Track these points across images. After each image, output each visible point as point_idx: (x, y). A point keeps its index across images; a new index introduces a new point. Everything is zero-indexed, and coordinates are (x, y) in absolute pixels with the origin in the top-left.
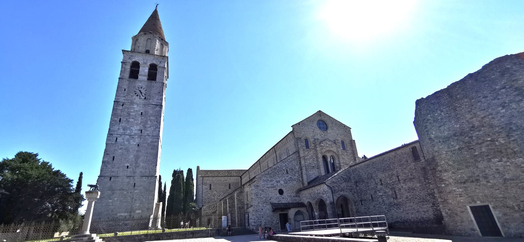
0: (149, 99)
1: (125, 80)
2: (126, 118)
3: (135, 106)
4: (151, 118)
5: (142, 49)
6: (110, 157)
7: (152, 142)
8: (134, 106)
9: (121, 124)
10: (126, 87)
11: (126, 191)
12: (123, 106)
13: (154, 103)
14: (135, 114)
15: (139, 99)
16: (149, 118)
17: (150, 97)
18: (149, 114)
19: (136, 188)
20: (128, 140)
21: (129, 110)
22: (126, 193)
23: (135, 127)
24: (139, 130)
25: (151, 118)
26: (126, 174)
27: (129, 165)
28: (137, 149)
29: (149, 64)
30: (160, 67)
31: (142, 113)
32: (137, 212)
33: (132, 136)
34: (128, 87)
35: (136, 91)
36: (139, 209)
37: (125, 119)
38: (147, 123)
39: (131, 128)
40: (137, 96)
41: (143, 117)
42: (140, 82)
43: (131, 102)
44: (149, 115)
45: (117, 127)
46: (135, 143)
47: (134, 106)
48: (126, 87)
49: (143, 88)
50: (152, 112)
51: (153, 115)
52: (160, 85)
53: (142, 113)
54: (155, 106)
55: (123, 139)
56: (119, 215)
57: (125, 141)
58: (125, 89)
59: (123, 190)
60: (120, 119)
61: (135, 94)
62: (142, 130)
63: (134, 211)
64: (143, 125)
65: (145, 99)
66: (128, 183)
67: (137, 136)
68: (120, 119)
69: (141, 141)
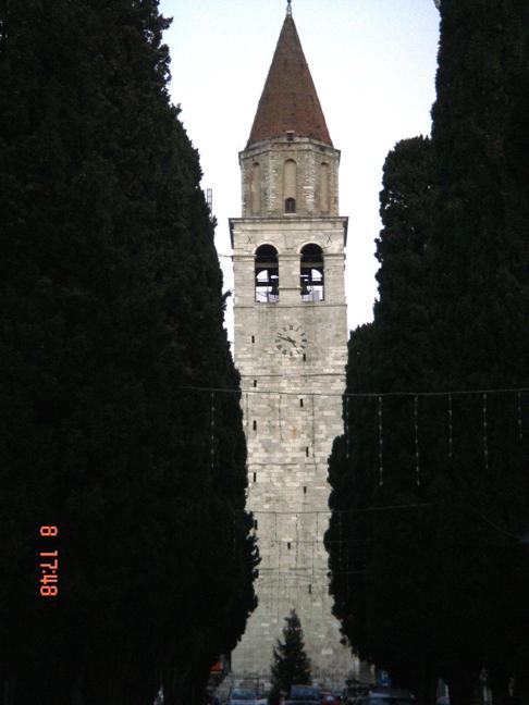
0: (317, 359)
1: (248, 310)
3: (284, 384)
4: (326, 413)
5: (275, 202)
8: (282, 385)
9: (258, 437)
10: (254, 330)
12: (255, 385)
13: (327, 371)
15: (289, 363)
17: (317, 353)
19: (314, 596)
20: (281, 479)
23: (291, 440)
24: (301, 449)
25: (326, 413)
27: (290, 540)
28: (301, 501)
29: (298, 251)
30: (329, 255)
32: (324, 652)
33: (289, 467)
34: (259, 331)
36: (327, 648)
37: (265, 423)
39: (283, 445)
40: (284, 352)
41: (304, 414)
42: (284, 310)
43: (273, 371)
46: (297, 485)
47: (282, 385)
48: (254, 330)
49: (295, 328)
52: (337, 313)
53: (301, 400)
54: (330, 377)
55: (269, 474)
57: (274, 480)
60: (255, 422)
61: (279, 347)
64: (308, 436)
65: (304, 358)
67: (298, 466)
68: (255, 422)
69: (309, 480)
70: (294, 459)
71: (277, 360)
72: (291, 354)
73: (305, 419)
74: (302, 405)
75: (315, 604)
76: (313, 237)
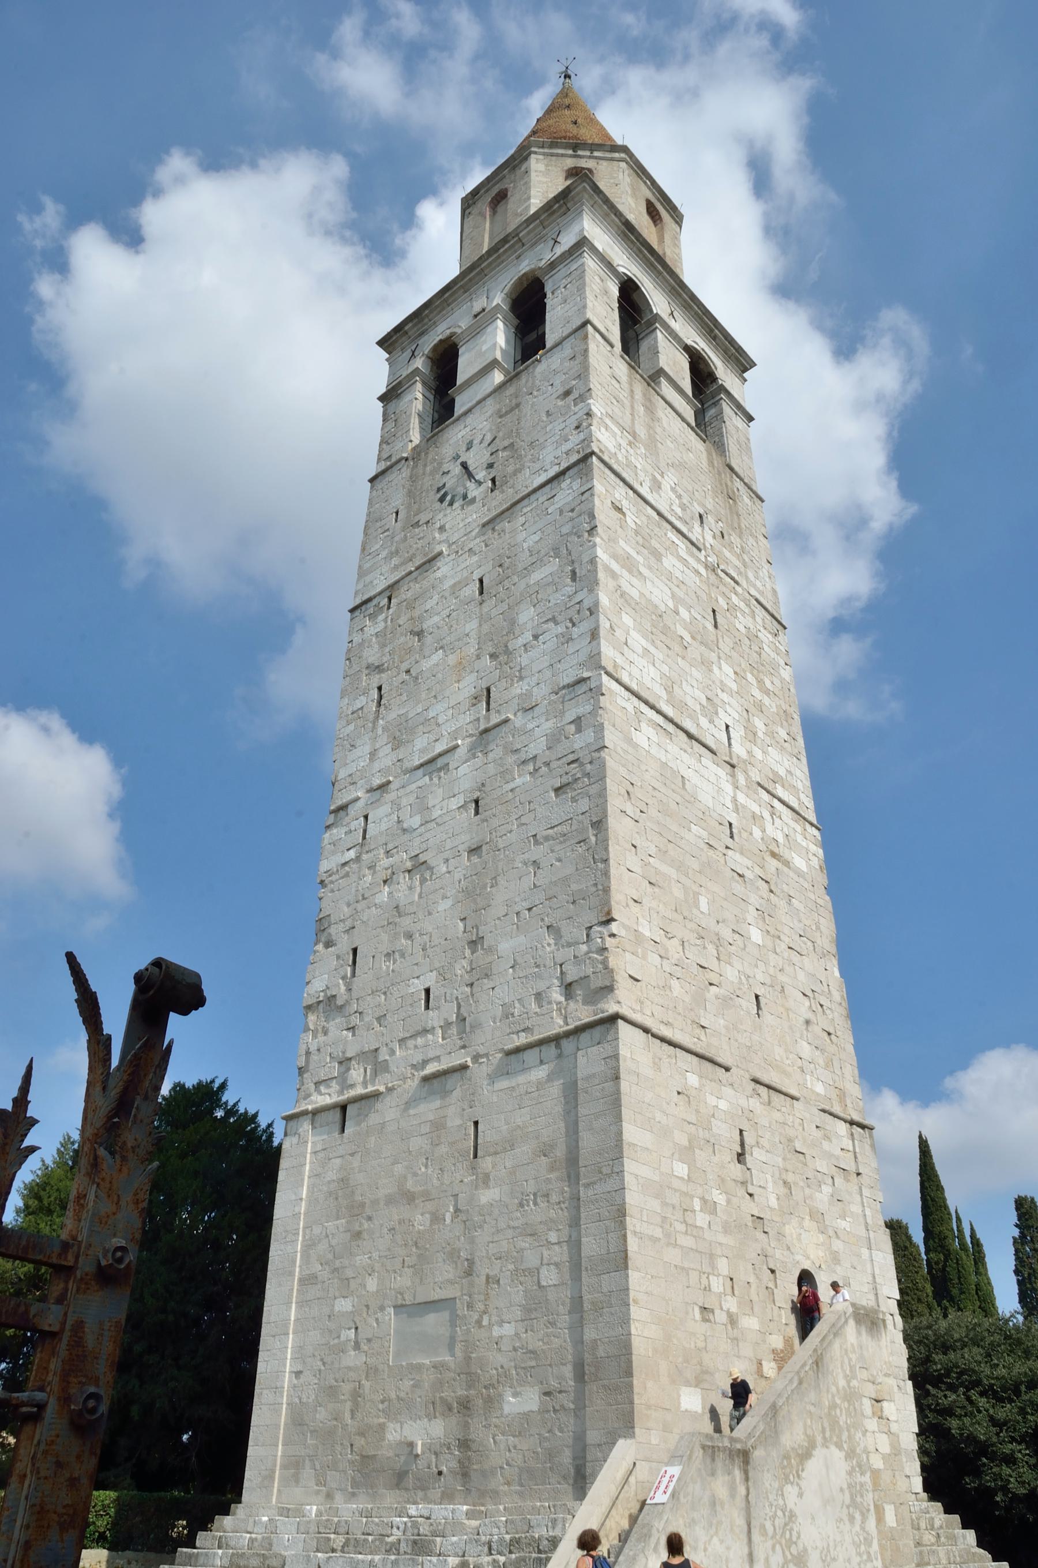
0: (516, 472)
2: (404, 666)
6: (338, 957)
7: (554, 739)
11: (430, 1206)
14: (447, 612)
16: (522, 585)
18: (524, 559)
19: (486, 1163)
20: (422, 807)
21: (416, 613)
22: (421, 1221)
26: (418, 1058)
27: (430, 980)
28: (466, 840)
31: (481, 581)
33: (440, 762)
35: (444, 485)
38: (513, 622)
39: (431, 714)
44: (520, 566)
45: (367, 749)
46: (460, 800)
50: (536, 538)
51: (543, 553)
53: (481, 581)
56: (393, 1434)
58: (397, 513)
59: (410, 1198)
60: (380, 688)
62: (488, 690)
63: (492, 1402)
66: (438, 1125)
67: (462, 752)
70: (454, 735)
71: (438, 525)
72: (465, 497)
73: (482, 619)
74: (481, 593)
75: (487, 1196)
76: (526, 262)
